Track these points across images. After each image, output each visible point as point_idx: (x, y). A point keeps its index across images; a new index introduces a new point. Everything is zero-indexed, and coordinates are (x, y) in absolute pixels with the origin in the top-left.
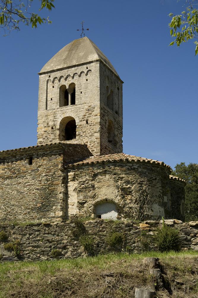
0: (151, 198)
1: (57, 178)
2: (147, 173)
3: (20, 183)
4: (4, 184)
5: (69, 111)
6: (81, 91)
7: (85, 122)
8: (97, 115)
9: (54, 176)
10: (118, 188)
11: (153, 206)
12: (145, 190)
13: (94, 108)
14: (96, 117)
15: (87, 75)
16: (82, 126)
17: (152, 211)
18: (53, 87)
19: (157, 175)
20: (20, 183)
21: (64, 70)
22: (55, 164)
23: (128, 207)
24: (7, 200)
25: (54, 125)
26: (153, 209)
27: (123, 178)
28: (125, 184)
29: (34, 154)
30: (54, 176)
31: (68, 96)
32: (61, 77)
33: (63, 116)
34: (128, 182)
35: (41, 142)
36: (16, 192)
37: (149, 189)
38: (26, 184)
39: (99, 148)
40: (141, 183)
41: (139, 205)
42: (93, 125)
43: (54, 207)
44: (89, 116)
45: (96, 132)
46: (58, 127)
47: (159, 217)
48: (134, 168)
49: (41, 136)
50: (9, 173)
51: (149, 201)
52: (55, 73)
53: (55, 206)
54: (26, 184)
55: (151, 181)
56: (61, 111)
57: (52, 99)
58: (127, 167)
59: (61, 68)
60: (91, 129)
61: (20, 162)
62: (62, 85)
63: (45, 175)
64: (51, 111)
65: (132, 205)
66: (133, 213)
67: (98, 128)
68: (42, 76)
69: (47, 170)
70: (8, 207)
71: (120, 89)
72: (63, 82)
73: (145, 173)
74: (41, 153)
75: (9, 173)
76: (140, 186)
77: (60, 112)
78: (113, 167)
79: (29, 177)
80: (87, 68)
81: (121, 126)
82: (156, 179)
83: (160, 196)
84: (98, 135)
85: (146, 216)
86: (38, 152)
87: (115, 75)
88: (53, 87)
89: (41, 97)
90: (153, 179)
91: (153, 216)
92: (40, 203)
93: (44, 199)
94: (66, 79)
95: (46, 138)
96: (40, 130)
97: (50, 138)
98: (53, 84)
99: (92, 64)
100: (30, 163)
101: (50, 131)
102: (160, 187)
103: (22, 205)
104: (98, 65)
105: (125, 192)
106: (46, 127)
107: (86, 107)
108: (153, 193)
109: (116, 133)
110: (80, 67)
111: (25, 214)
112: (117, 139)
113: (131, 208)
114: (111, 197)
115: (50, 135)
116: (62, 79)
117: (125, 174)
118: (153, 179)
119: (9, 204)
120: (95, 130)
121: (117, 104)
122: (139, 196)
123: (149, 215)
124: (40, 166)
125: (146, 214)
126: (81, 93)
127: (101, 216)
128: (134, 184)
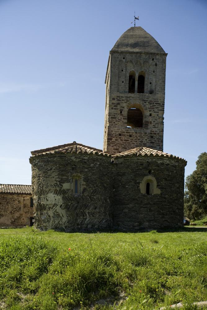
0: (46, 188)
2: (43, 166)
11: (47, 195)
17: (47, 200)
19: (53, 165)
26: (48, 198)
37: (44, 180)
41: (37, 196)
51: (45, 191)
55: (46, 172)
71: (164, 62)
73: (42, 166)
81: (160, 104)
82: (51, 169)
83: (55, 185)
87: (147, 53)
102: (56, 176)
108: (48, 184)
112: (150, 119)
118: (49, 170)
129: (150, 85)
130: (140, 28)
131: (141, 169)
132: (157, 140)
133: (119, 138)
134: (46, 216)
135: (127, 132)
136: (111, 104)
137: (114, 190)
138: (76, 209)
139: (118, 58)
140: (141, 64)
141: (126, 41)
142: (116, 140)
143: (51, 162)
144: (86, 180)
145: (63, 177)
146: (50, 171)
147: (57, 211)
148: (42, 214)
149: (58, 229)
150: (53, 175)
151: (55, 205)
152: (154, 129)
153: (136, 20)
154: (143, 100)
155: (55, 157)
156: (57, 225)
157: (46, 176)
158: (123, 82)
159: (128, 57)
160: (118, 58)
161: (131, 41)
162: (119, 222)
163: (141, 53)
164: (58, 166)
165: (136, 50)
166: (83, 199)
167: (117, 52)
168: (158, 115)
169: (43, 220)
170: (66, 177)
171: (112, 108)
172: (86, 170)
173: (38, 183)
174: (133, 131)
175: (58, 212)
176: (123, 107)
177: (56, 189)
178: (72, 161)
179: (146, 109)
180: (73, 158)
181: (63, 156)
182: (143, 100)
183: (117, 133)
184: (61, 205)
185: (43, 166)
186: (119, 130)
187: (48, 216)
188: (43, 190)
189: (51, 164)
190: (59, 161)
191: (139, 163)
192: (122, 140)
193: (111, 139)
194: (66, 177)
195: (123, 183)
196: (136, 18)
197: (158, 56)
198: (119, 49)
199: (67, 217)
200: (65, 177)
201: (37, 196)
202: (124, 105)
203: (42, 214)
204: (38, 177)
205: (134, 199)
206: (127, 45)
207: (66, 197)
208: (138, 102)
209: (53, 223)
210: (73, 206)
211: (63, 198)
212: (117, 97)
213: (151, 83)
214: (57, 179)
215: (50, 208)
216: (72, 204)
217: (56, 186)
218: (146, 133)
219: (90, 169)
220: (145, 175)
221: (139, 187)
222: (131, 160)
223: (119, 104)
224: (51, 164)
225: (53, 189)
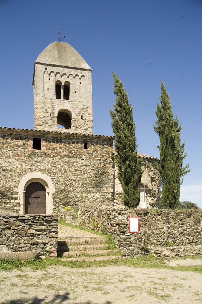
1: (108, 163)
3: (77, 162)
4: (62, 161)
6: (76, 91)
7: (80, 117)
8: (90, 114)
9: (106, 161)
13: (88, 108)
14: (90, 115)
15: (80, 79)
16: (78, 120)
18: (49, 79)
20: (77, 162)
21: (61, 68)
22: (106, 152)
24: (66, 175)
27: (153, 170)
28: (153, 175)
29: (89, 140)
30: (106, 161)
31: (63, 91)
32: (58, 73)
33: (61, 108)
35: (41, 124)
36: (73, 169)
38: (83, 164)
42: (87, 122)
43: (106, 185)
44: (84, 113)
45: (89, 127)
49: (41, 119)
50: (66, 152)
52: (52, 67)
53: (107, 184)
54: (83, 164)
56: (59, 102)
57: (48, 90)
59: (57, 65)
60: (86, 124)
61: (77, 145)
62: (58, 80)
63: (99, 160)
64: (49, 100)
69: (100, 155)
70: (67, 181)
72: (58, 78)
74: (95, 141)
75: (66, 152)
77: (58, 103)
78: (147, 162)
79: (85, 159)
80: (81, 73)
86: (92, 140)
88: (49, 79)
89: (39, 84)
92: (94, 181)
93: (98, 178)
94: (62, 76)
95: (45, 122)
96: (39, 114)
97: (49, 123)
98: (50, 76)
99: (85, 71)
100: (86, 147)
101: (49, 117)
103: (79, 181)
106: (44, 112)
107: (81, 105)
111: (83, 188)
115: (49, 120)
116: (58, 75)
117: (154, 168)
119: (67, 178)
120: (89, 126)
124: (94, 151)
126: (76, 92)
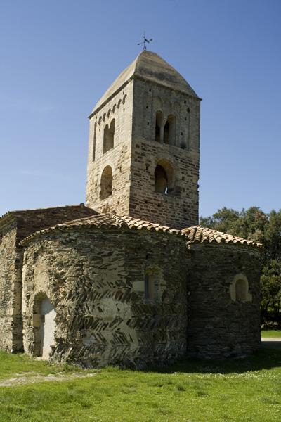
0: (99, 288)
2: (92, 246)
5: (110, 159)
10: (51, 275)
11: (101, 301)
12: (87, 276)
15: (124, 103)
23: (60, 305)
25: (97, 181)
26: (102, 307)
27: (55, 258)
34: (61, 264)
37: (93, 273)
39: (128, 205)
40: (80, 266)
45: (127, 182)
46: (100, 182)
47: (116, 319)
48: (71, 240)
51: (95, 295)
55: (100, 258)
58: (61, 239)
65: (64, 302)
66: (66, 315)
67: (128, 174)
68: (92, 118)
71: (198, 109)
73: (89, 247)
76: (78, 270)
82: (110, 254)
84: (128, 185)
85: (88, 319)
87: (179, 92)
90: (105, 256)
91: (102, 319)
104: (133, 84)
105: (58, 279)
108: (103, 279)
109: (180, 176)
110: (118, 95)
112: (183, 185)
113: (63, 306)
114: (45, 289)
117: (59, 251)
118: (105, 256)
121: (186, 133)
122: (75, 286)
123: (92, 318)
125: (88, 317)
127: (44, 316)
128: (69, 266)
129: (181, 136)
130: (155, 54)
131: (230, 263)
132: (191, 216)
133: (145, 207)
134: (96, 339)
135: (155, 200)
136: (134, 153)
137: (189, 293)
138: (152, 327)
139: (143, 87)
140: (171, 104)
141: (147, 67)
142: (141, 209)
143: (111, 241)
144: (167, 276)
145: (132, 270)
146: (107, 258)
147: (121, 331)
148: (85, 336)
149: (124, 364)
150: (115, 265)
151: (118, 320)
152: (188, 200)
153: (146, 43)
154: (175, 156)
155: (120, 233)
156: (120, 356)
157: (99, 265)
158: (148, 124)
159: (155, 89)
160: (143, 87)
161: (154, 69)
162: (200, 345)
163: (171, 90)
164: (123, 249)
165: (165, 83)
166: (163, 309)
167: (142, 79)
168: (192, 180)
169: (88, 348)
170: (138, 271)
171: (136, 160)
172: (166, 260)
173: (77, 276)
174: (163, 199)
175: (122, 334)
176: (150, 161)
177: (121, 292)
178: (148, 242)
179: (178, 170)
180: (149, 238)
181: (133, 233)
182: (175, 156)
183: (143, 199)
184: (129, 321)
185: (92, 246)
186: (144, 194)
187: (101, 341)
188: (90, 290)
189: (110, 245)
190: (126, 241)
191: (228, 255)
192: (148, 210)
193: (134, 207)
194: (138, 271)
195: (205, 283)
196: (146, 40)
197: (190, 101)
198: (144, 76)
199: (139, 341)
200: (135, 271)
201: (72, 300)
202: (152, 158)
203: (85, 336)
204: (77, 265)
205: (221, 309)
206: (151, 73)
207: (136, 305)
208: (168, 157)
209: (113, 352)
210: (149, 322)
211: (134, 308)
212: (143, 144)
213: (182, 134)
214: (123, 273)
215: (105, 325)
216: (147, 317)
217: (118, 285)
218: (178, 204)
219: (170, 258)
220: (236, 273)
221: (228, 290)
222: (216, 248)
223: (145, 155)
224: (110, 245)
225: (113, 291)
